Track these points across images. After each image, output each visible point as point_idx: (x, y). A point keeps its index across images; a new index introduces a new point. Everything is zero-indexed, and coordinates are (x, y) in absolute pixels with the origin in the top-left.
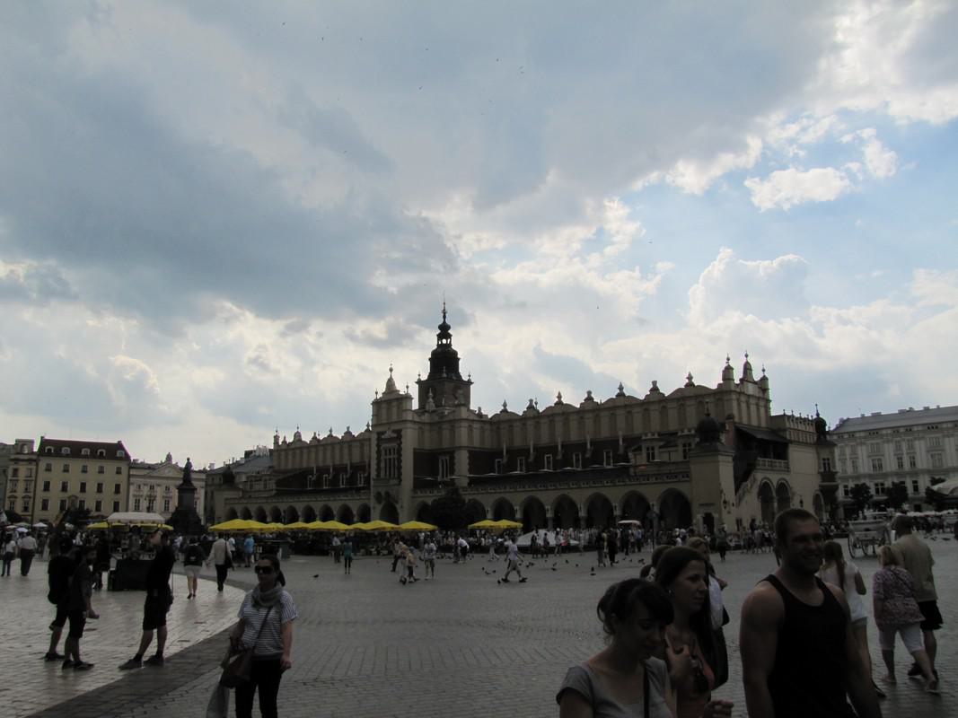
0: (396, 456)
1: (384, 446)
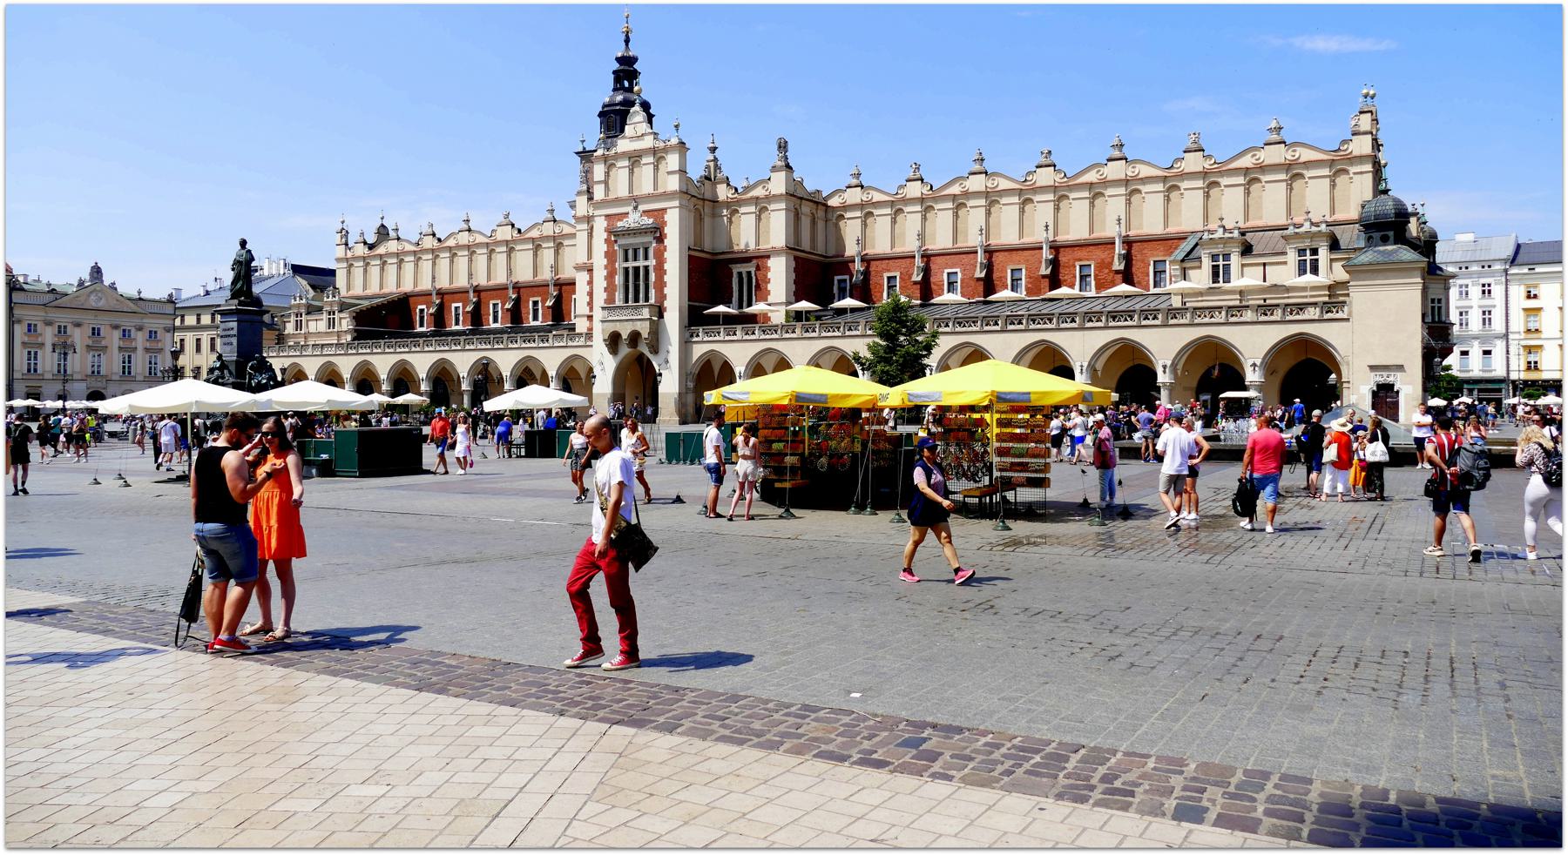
0: (652, 262)
1: (622, 241)
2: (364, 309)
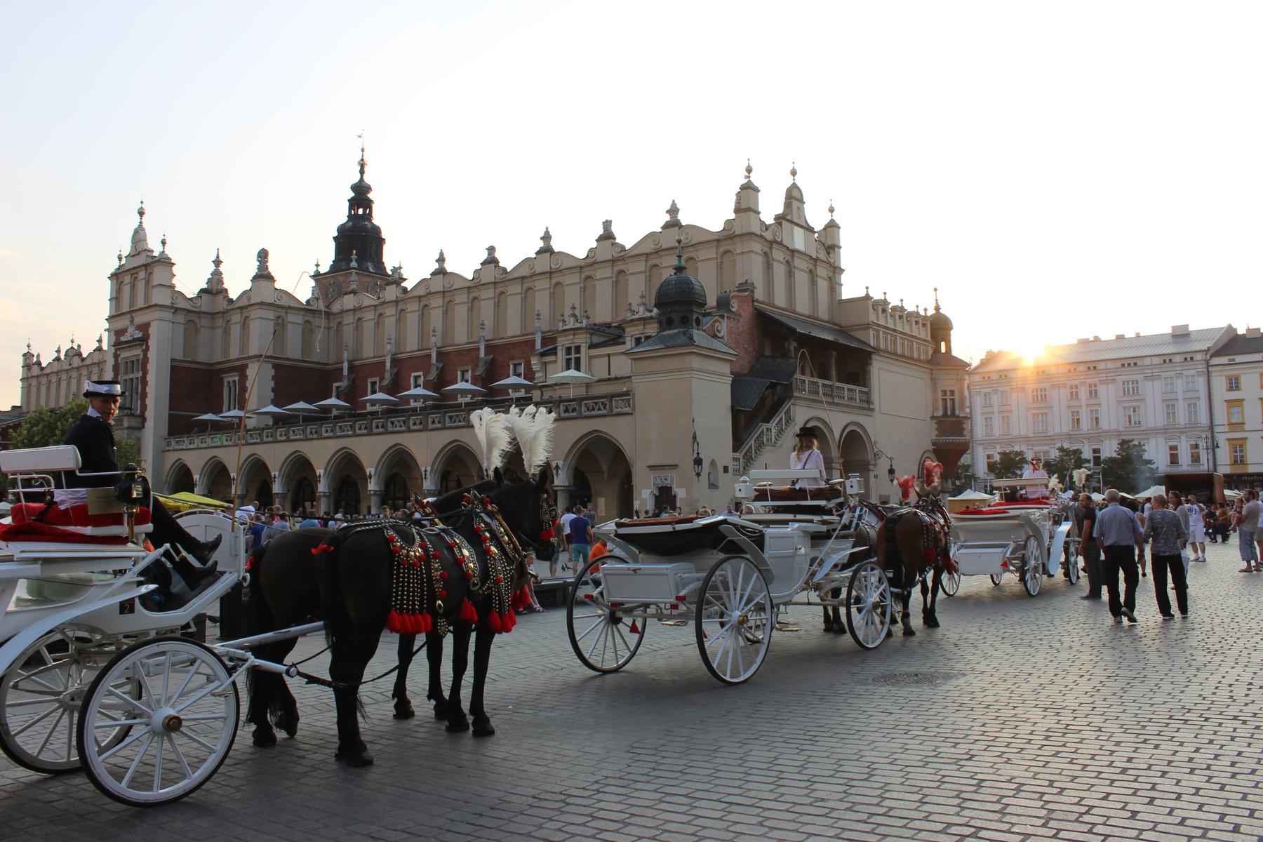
0: (140, 374)
1: (124, 354)
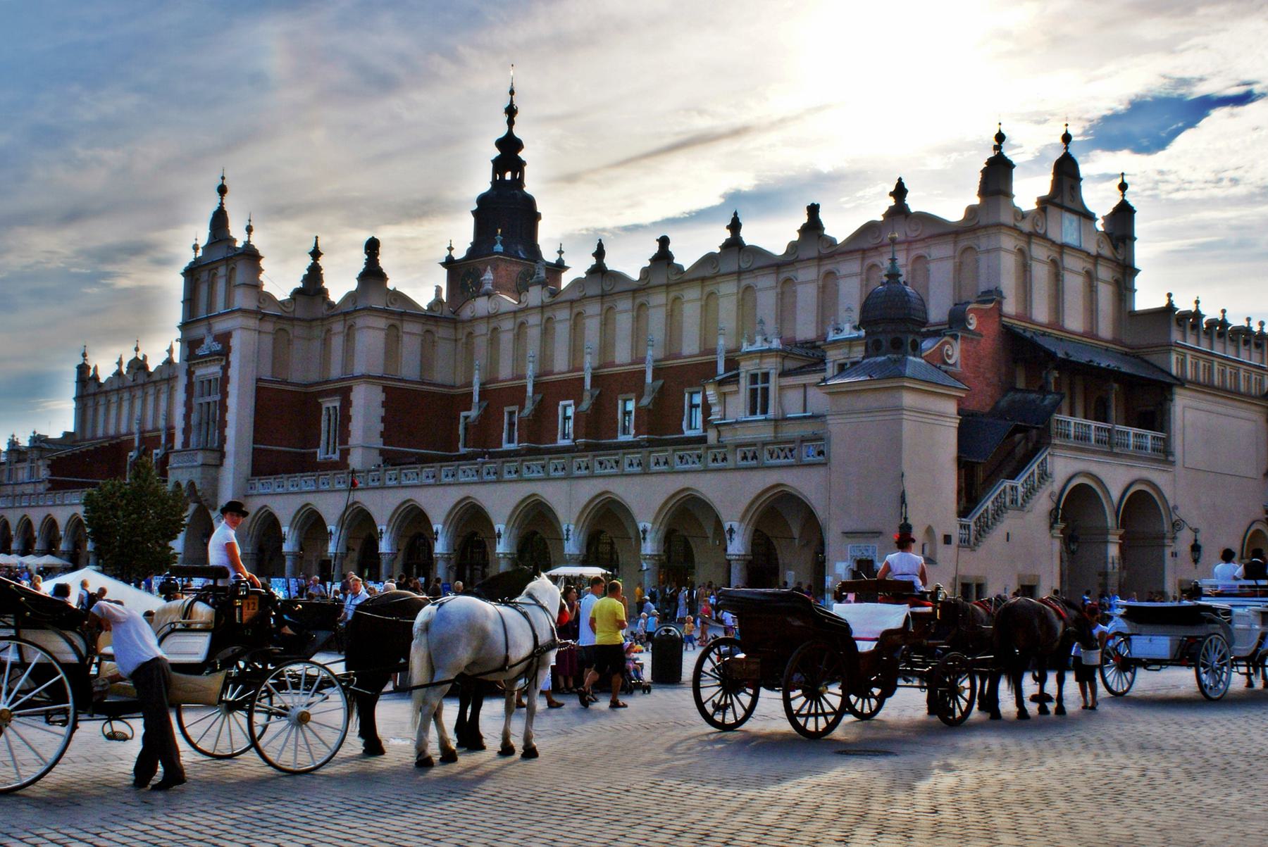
0: (217, 398)
2: (64, 456)
